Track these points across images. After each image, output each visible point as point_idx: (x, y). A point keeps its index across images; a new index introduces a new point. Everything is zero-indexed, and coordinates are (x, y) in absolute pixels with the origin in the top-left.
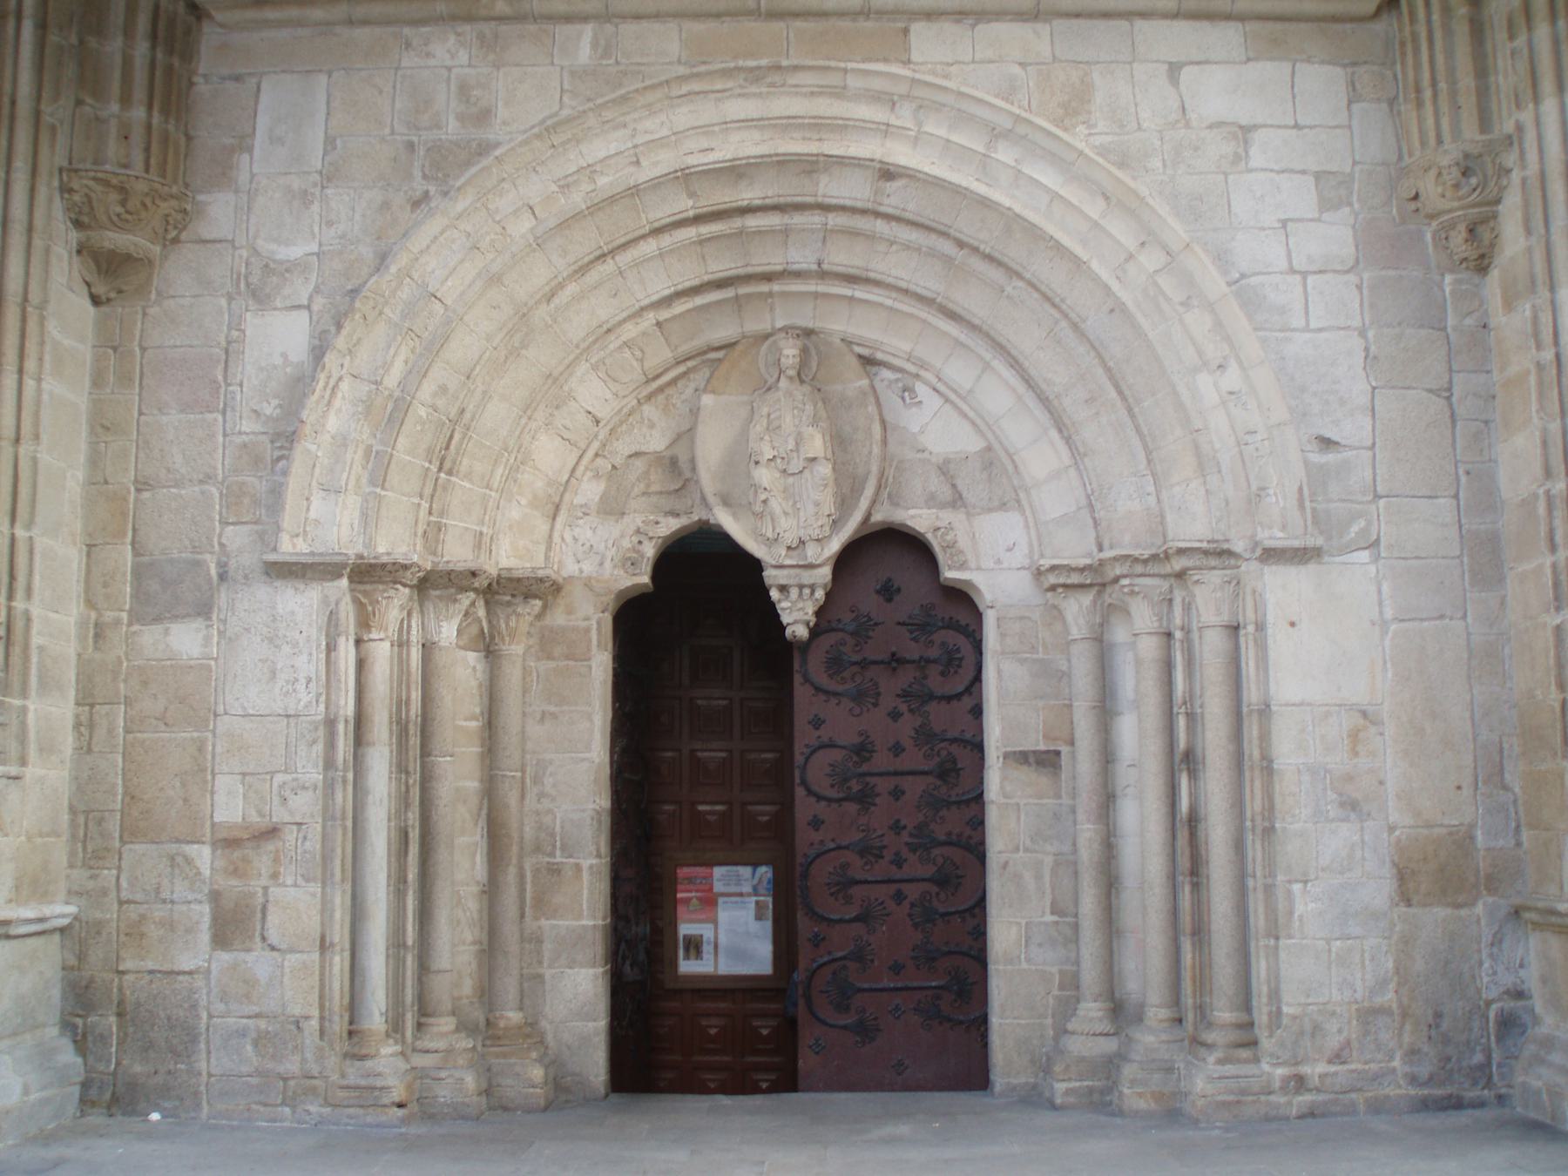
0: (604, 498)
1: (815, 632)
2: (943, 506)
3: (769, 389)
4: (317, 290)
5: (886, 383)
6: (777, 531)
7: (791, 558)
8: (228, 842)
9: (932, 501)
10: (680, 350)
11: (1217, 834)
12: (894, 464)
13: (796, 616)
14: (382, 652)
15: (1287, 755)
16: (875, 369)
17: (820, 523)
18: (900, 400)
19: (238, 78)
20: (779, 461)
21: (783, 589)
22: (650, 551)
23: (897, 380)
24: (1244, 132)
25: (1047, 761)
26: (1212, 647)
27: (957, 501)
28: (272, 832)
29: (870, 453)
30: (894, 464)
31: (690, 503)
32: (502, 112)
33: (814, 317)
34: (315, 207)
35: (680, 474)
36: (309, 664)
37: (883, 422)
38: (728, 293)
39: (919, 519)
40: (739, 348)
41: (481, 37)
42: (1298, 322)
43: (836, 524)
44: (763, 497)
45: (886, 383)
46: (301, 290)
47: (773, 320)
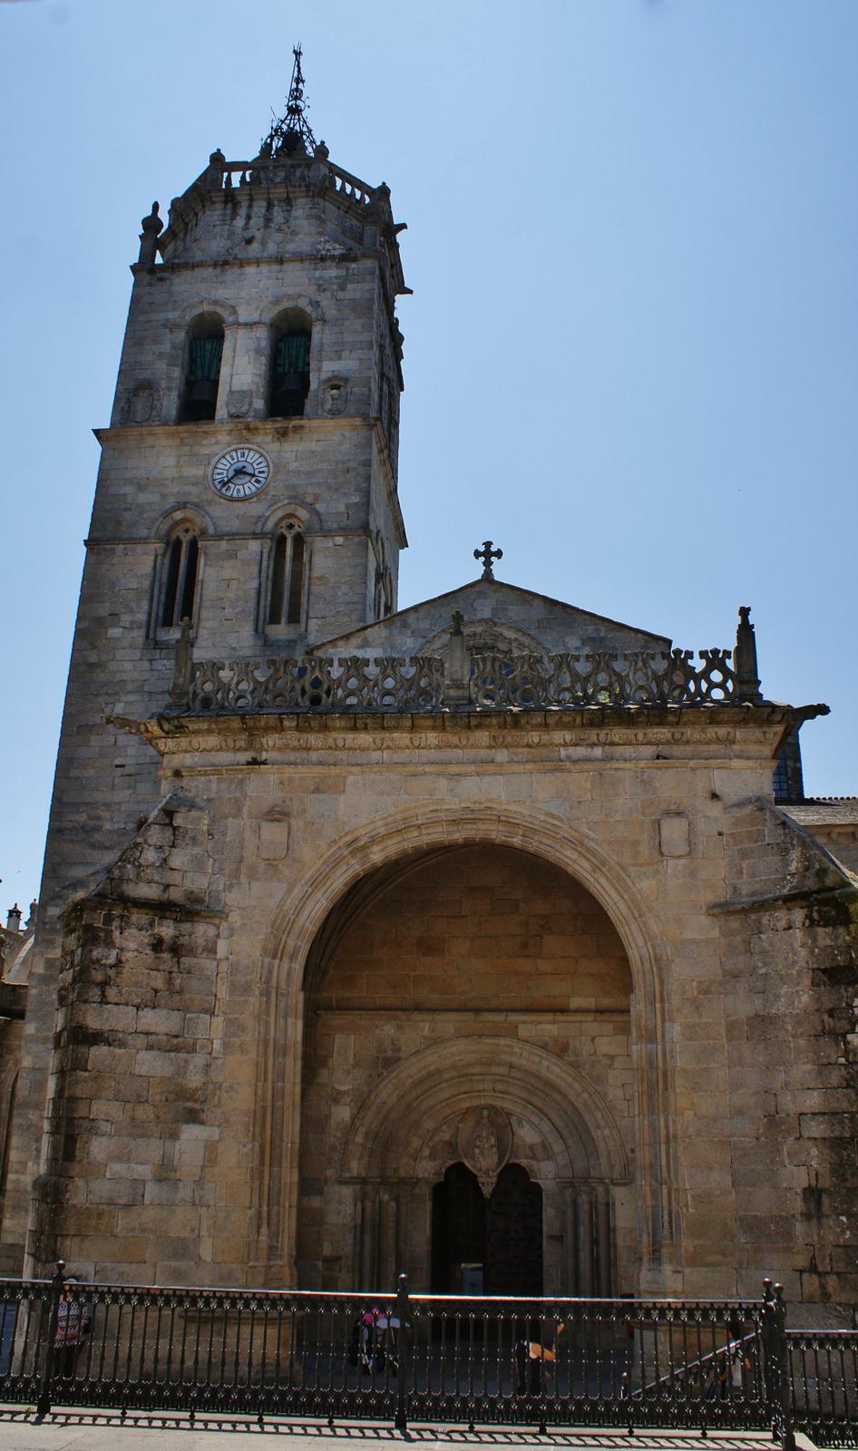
0: (430, 1153)
1: (492, 1196)
2: (530, 1158)
4: (352, 1100)
8: (327, 1260)
9: (526, 1157)
11: (603, 1264)
13: (487, 1191)
14: (368, 1204)
15: (620, 1242)
19: (328, 1035)
21: (483, 1184)
22: (444, 1170)
24: (612, 1058)
25: (559, 1239)
26: (602, 1208)
27: (534, 1157)
28: (339, 1258)
32: (403, 1048)
34: (351, 1076)
36: (349, 1209)
37: (513, 1133)
38: (467, 1095)
39: (523, 1162)
41: (397, 1025)
42: (626, 1114)
43: (499, 1164)
46: (347, 1099)
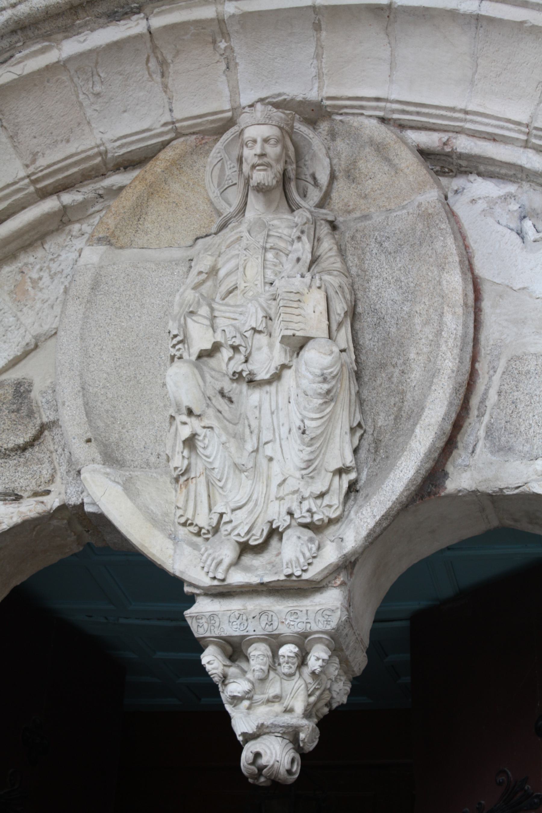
3: (223, 227)
5: (481, 205)
6: (219, 508)
7: (247, 569)
10: (42, 162)
12: (502, 364)
16: (458, 182)
17: (319, 487)
18: (514, 236)
20: (226, 353)
23: (507, 198)
29: (439, 333)
30: (502, 364)
31: (46, 474)
33: (319, 76)
35: (31, 414)
40: (167, 155)
44: (185, 432)
45: (481, 205)
47: (234, 92)
